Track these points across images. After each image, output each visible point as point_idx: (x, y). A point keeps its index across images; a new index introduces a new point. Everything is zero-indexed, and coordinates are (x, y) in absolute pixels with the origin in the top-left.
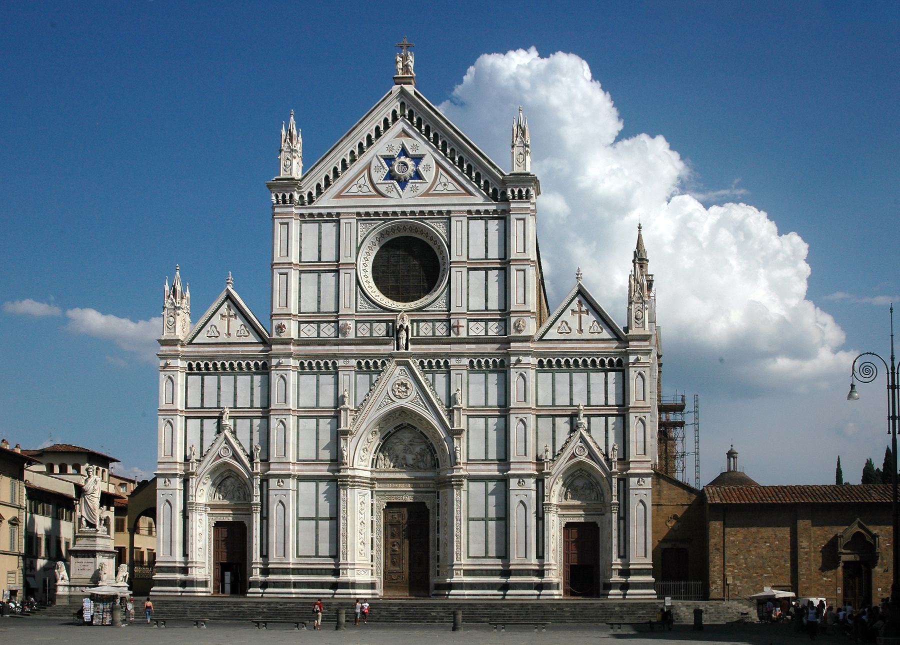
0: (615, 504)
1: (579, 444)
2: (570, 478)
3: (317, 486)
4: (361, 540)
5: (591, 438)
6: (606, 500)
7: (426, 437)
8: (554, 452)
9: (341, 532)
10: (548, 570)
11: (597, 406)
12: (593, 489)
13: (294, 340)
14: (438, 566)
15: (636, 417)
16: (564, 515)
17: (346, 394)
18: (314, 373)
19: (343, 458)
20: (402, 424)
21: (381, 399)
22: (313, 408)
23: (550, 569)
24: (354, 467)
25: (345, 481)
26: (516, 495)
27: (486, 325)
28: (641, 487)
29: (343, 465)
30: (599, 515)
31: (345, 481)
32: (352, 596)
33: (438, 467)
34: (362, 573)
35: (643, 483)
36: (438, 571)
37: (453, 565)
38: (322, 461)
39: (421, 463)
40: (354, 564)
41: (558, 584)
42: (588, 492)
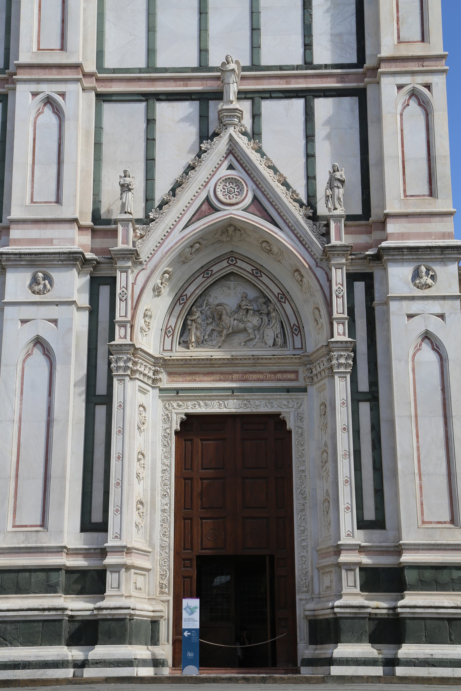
0: (343, 345)
1: (224, 172)
2: (200, 280)
5: (263, 155)
6: (311, 347)
8: (149, 199)
10: (117, 568)
11: (281, 68)
12: (268, 314)
15: (400, 87)
16: (177, 391)
23: (128, 568)
26: (24, 322)
28: (426, 293)
30: (288, 390)
35: (430, 281)
41: (155, 623)
42: (255, 321)
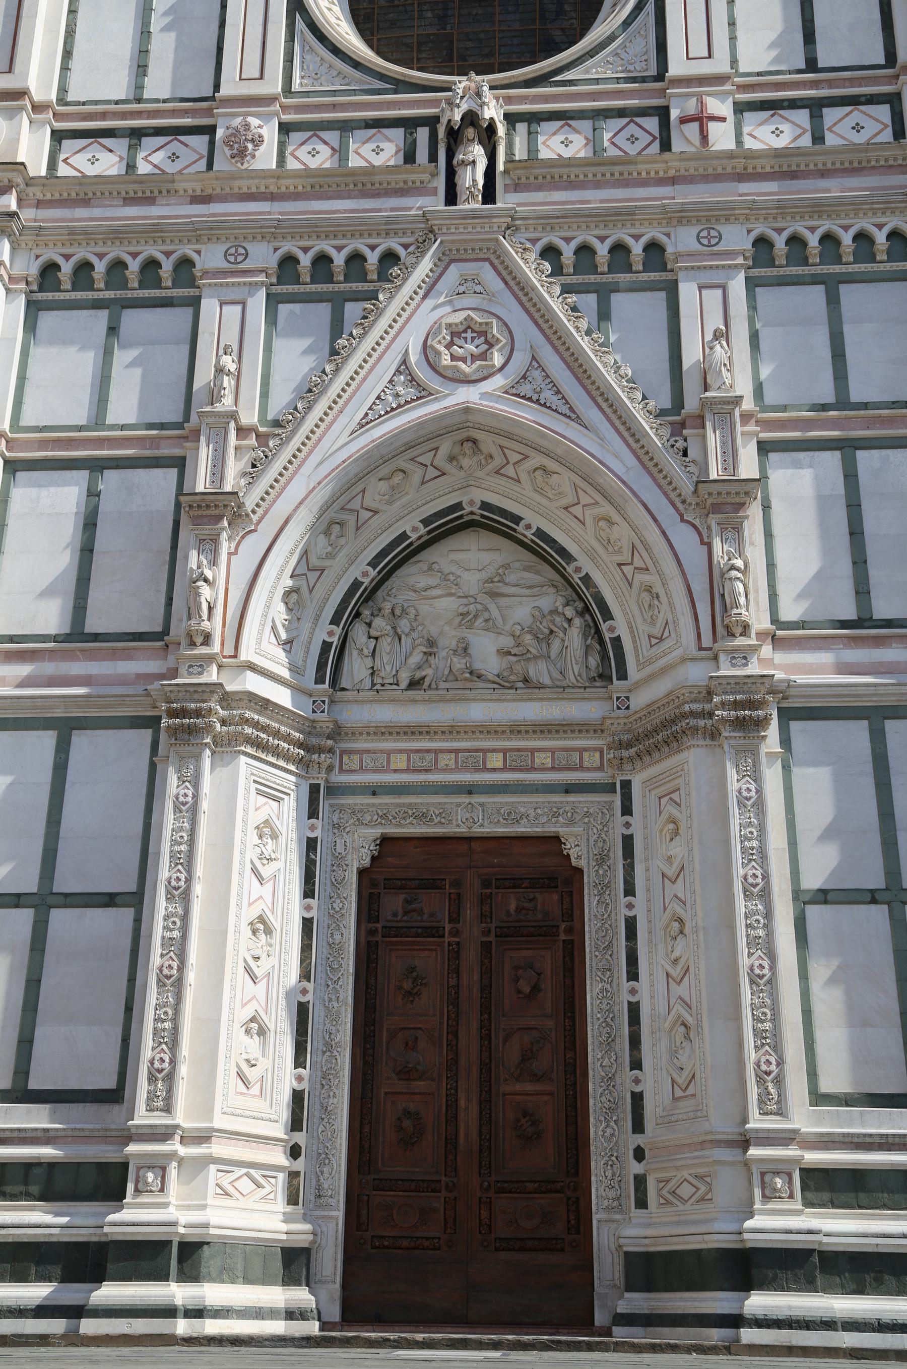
3: (63, 749)
4: (248, 1013)
7: (563, 552)
9: (156, 960)
13: (30, 182)
14: (639, 1154)
17: (229, 362)
18: (97, 305)
19: (192, 611)
20: (458, 506)
21: (377, 382)
22: (80, 428)
24: (244, 656)
25: (198, 713)
27: (816, 117)
29: (193, 644)
31: (198, 713)
32: (182, 1327)
33: (623, 676)
34: (245, 1185)
36: (640, 1182)
37: (745, 1143)
38: (96, 637)
39: (542, 665)
40: (203, 1137)
